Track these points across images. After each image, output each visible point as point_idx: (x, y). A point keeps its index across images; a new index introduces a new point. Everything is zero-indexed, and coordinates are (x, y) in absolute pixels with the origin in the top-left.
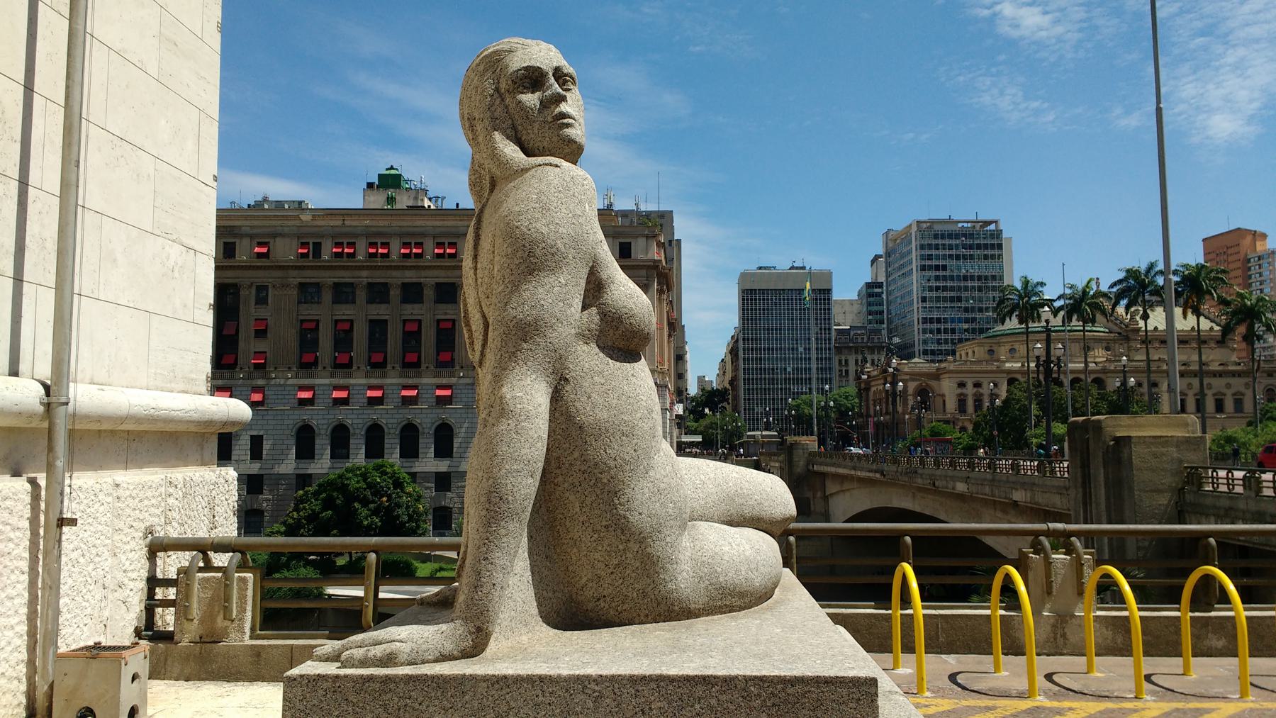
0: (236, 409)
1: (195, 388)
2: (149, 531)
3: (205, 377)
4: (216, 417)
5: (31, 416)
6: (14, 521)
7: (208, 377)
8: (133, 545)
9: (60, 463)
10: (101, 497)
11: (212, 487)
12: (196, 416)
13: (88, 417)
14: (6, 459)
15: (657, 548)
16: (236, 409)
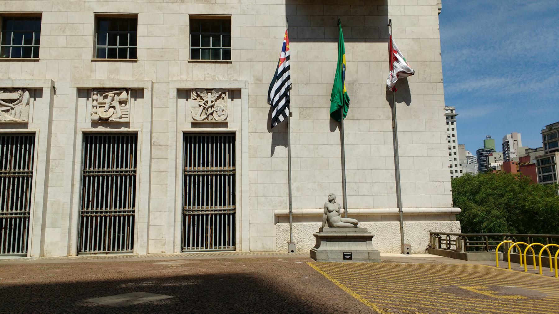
0: (458, 210)
1: (447, 206)
2: (430, 231)
3: (450, 204)
4: (447, 212)
5: (398, 213)
6: (397, 227)
7: (451, 204)
8: (425, 232)
9: (401, 220)
10: (416, 225)
11: (450, 224)
12: (440, 212)
13: (406, 213)
14: (397, 219)
15: (332, 223)
16: (458, 210)
